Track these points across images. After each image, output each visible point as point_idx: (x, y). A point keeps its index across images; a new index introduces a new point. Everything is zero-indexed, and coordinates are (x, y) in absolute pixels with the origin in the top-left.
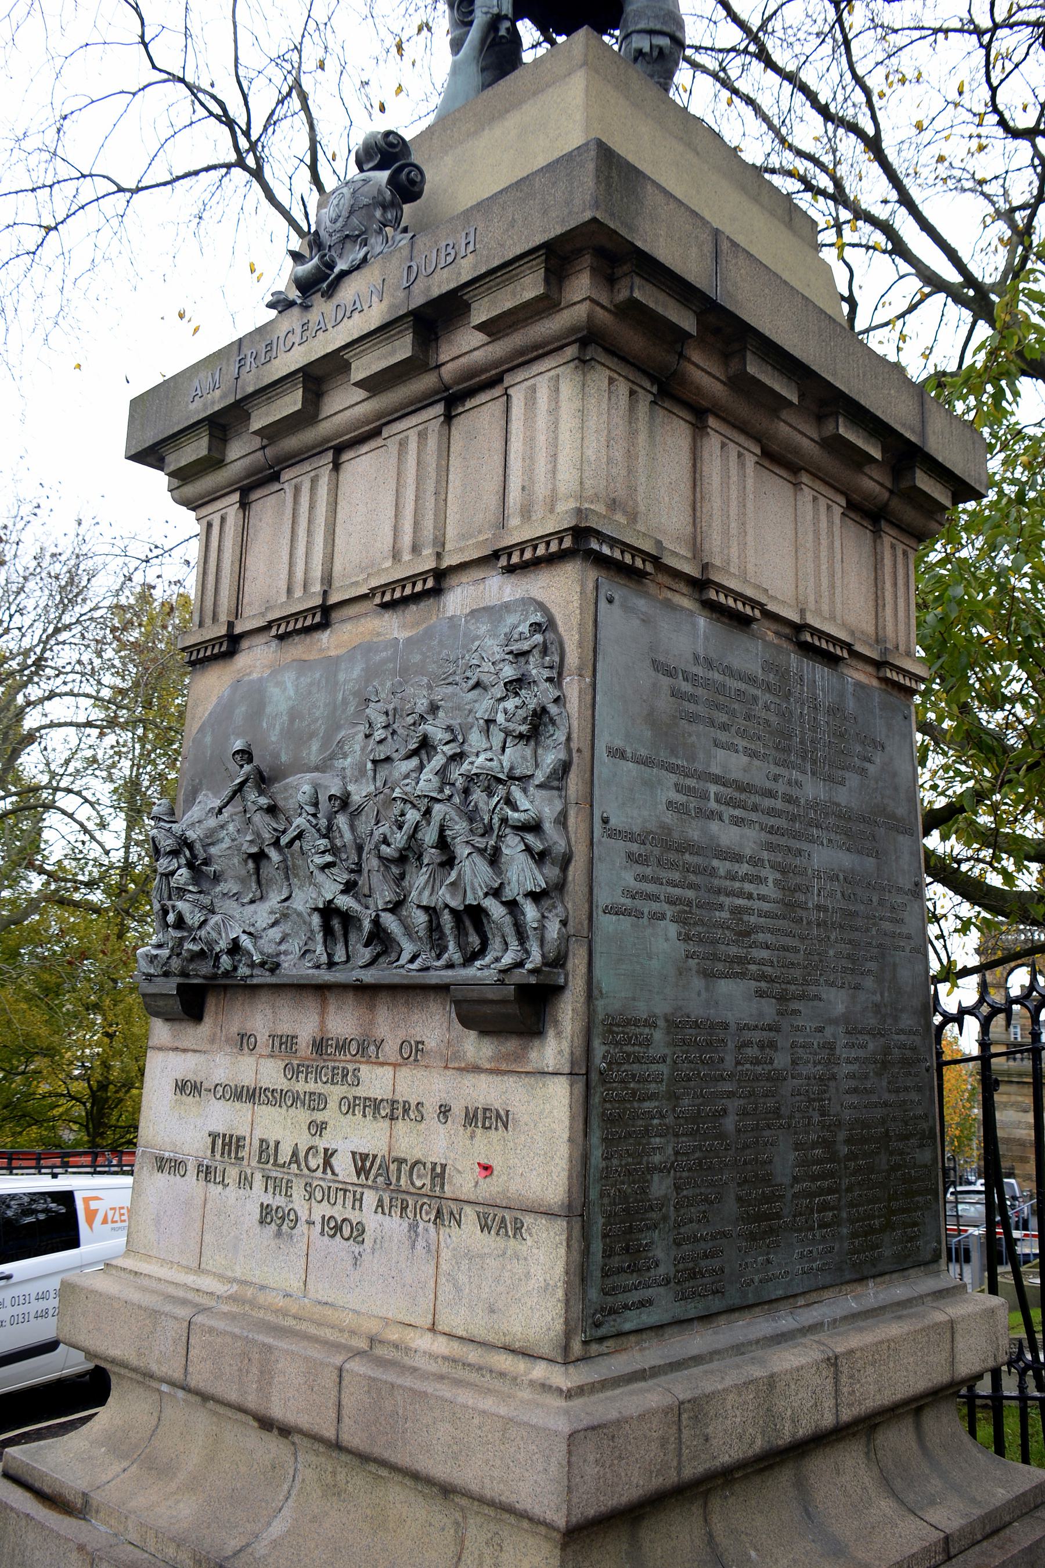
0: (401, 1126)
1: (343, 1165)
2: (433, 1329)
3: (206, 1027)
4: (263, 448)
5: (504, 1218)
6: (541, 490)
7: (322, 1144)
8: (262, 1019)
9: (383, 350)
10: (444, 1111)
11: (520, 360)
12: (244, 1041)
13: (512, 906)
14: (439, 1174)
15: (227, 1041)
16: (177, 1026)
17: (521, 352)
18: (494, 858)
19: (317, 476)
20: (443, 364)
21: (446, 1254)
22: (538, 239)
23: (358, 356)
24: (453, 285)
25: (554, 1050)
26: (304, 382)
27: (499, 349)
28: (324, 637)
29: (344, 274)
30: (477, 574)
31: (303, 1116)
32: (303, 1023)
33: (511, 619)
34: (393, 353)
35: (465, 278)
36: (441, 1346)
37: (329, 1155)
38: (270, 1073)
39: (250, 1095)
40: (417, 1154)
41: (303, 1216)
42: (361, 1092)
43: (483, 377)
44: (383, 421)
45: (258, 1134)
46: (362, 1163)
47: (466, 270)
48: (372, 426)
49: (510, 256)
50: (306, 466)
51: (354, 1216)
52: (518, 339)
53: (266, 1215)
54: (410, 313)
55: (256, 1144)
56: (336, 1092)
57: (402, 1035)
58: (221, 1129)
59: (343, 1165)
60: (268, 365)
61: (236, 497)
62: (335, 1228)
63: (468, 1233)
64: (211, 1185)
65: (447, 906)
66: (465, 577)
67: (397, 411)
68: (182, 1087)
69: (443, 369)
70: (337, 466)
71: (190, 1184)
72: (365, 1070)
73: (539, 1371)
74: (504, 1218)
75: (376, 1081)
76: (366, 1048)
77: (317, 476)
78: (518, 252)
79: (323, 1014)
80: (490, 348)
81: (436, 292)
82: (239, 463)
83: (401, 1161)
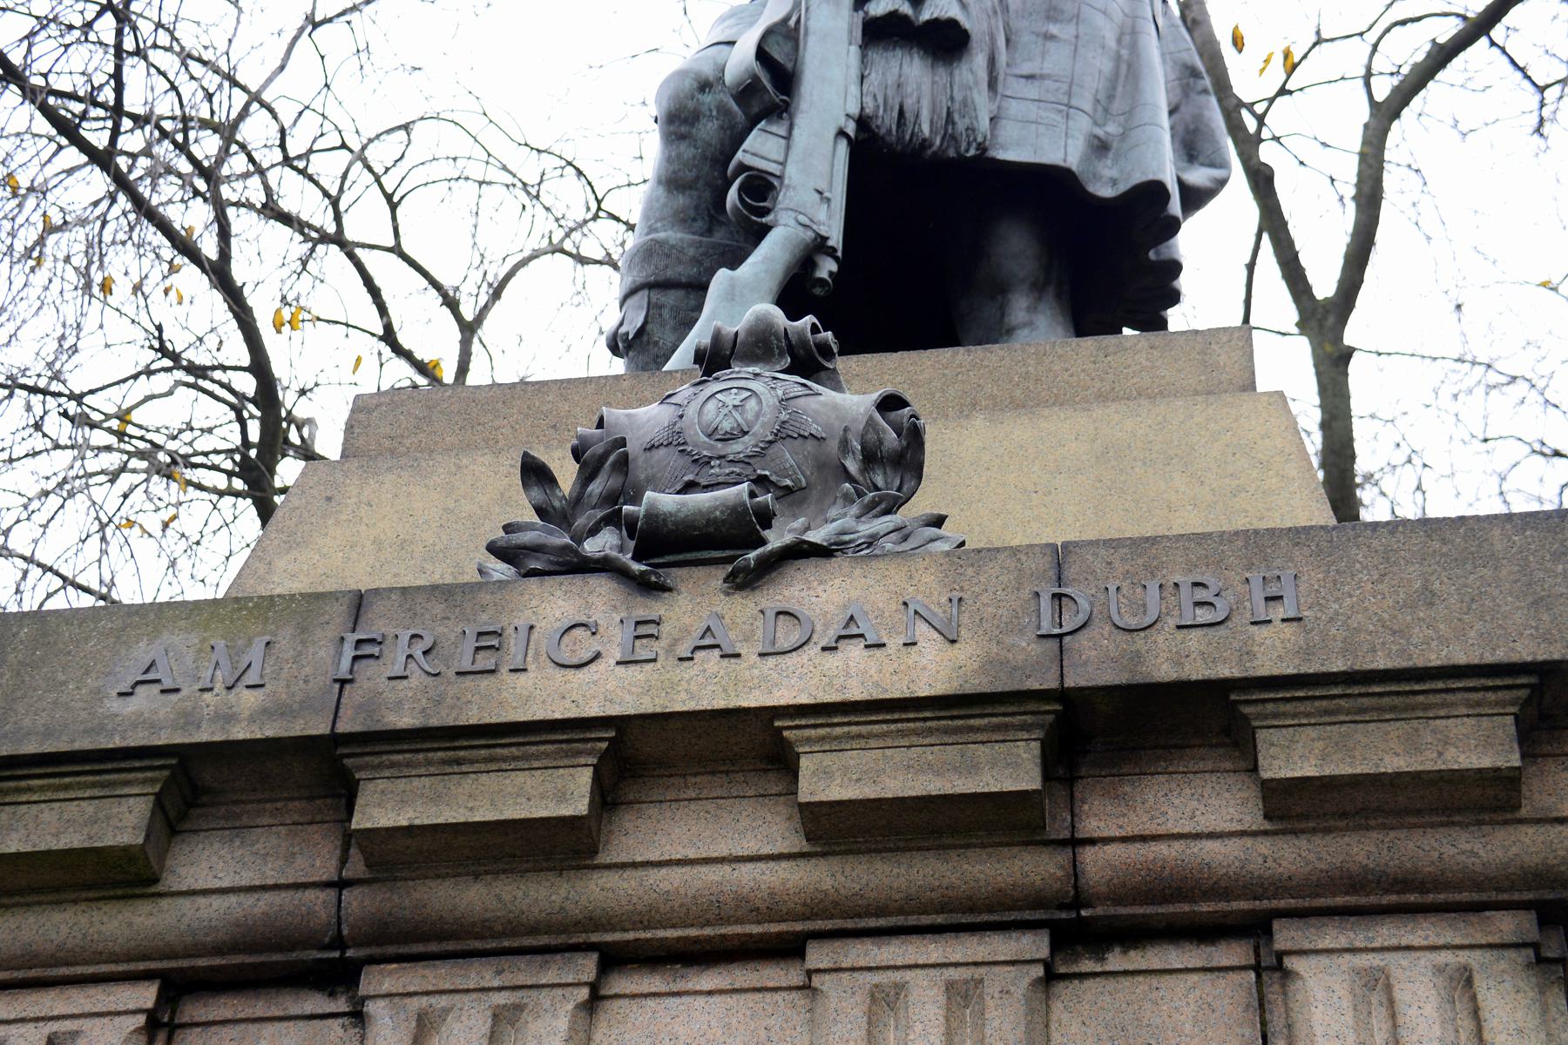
4: (340, 885)
9: (930, 755)
11: (1340, 900)
17: (1356, 882)
19: (519, 1007)
20: (1092, 842)
22: (1524, 651)
23: (836, 746)
24: (1225, 671)
26: (604, 756)
27: (1291, 856)
29: (801, 551)
34: (974, 768)
35: (1266, 666)
43: (1205, 907)
44: (819, 925)
47: (1273, 652)
48: (775, 928)
49: (1434, 659)
50: (481, 974)
52: (1359, 850)
54: (1062, 695)
60: (485, 682)
61: (146, 995)
67: (881, 911)
69: (1088, 855)
70: (596, 999)
77: (519, 1007)
78: (1461, 658)
80: (1263, 846)
81: (1164, 672)
82: (218, 903)
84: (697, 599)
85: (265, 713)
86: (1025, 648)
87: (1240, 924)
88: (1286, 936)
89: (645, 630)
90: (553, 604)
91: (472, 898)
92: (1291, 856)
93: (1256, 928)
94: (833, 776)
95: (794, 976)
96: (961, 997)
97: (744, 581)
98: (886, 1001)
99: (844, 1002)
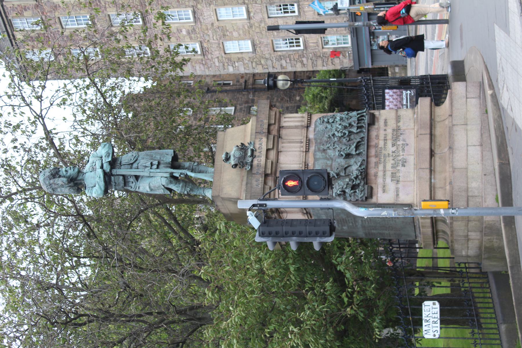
0: (388, 138)
1: (394, 149)
2: (414, 129)
3: (373, 186)
5: (398, 119)
6: (300, 119)
7: (391, 154)
8: (372, 171)
10: (385, 130)
12: (376, 176)
13: (358, 114)
14: (394, 130)
15: (376, 179)
16: (373, 194)
18: (351, 117)
21: (404, 128)
25: (376, 113)
28: (310, 165)
30: (309, 132)
31: (387, 159)
32: (373, 160)
33: (317, 124)
35: (267, 122)
36: (416, 127)
37: (393, 152)
38: (381, 167)
39: (385, 171)
40: (391, 134)
41: (402, 157)
42: (383, 147)
45: (390, 169)
46: (393, 145)
47: (266, 122)
51: (401, 145)
53: (403, 165)
55: (392, 169)
56: (383, 152)
57: (375, 139)
58: (390, 179)
59: (394, 149)
62: (403, 150)
63: (400, 124)
64: (400, 180)
65: (358, 124)
66: (308, 134)
68: (384, 191)
71: (400, 185)
72: (380, 146)
73: (416, 111)
74: (398, 119)
75: (381, 143)
76: (376, 146)
79: (371, 157)
83: (393, 138)
84: (256, 154)
85: (262, 178)
86: (264, 134)
87: (280, 128)
88: (281, 126)
89: (258, 156)
90: (255, 162)
91: (274, 169)
92: (277, 124)
93: (280, 127)
94: (271, 146)
95: (280, 153)
96: (283, 143)
97: (256, 150)
98: (282, 147)
99: (282, 149)
